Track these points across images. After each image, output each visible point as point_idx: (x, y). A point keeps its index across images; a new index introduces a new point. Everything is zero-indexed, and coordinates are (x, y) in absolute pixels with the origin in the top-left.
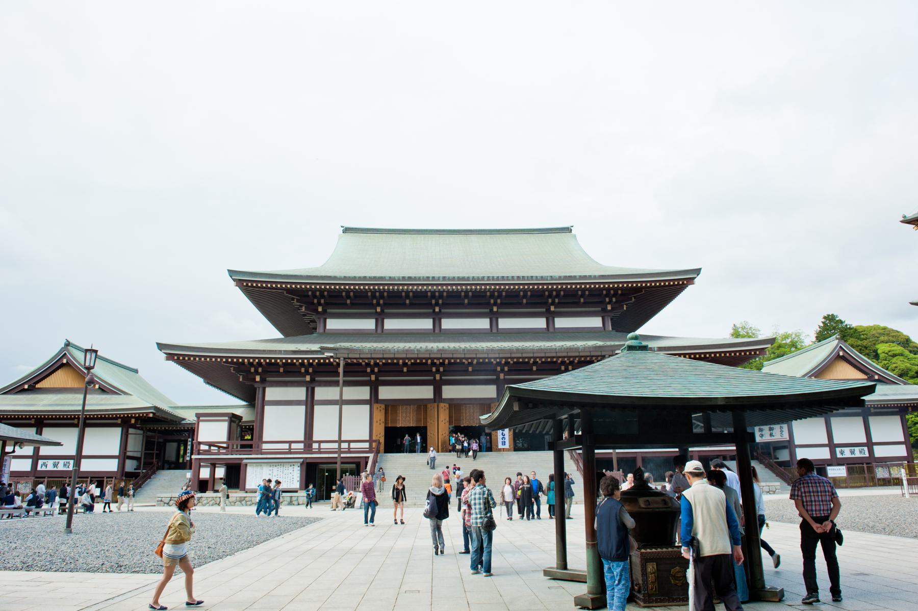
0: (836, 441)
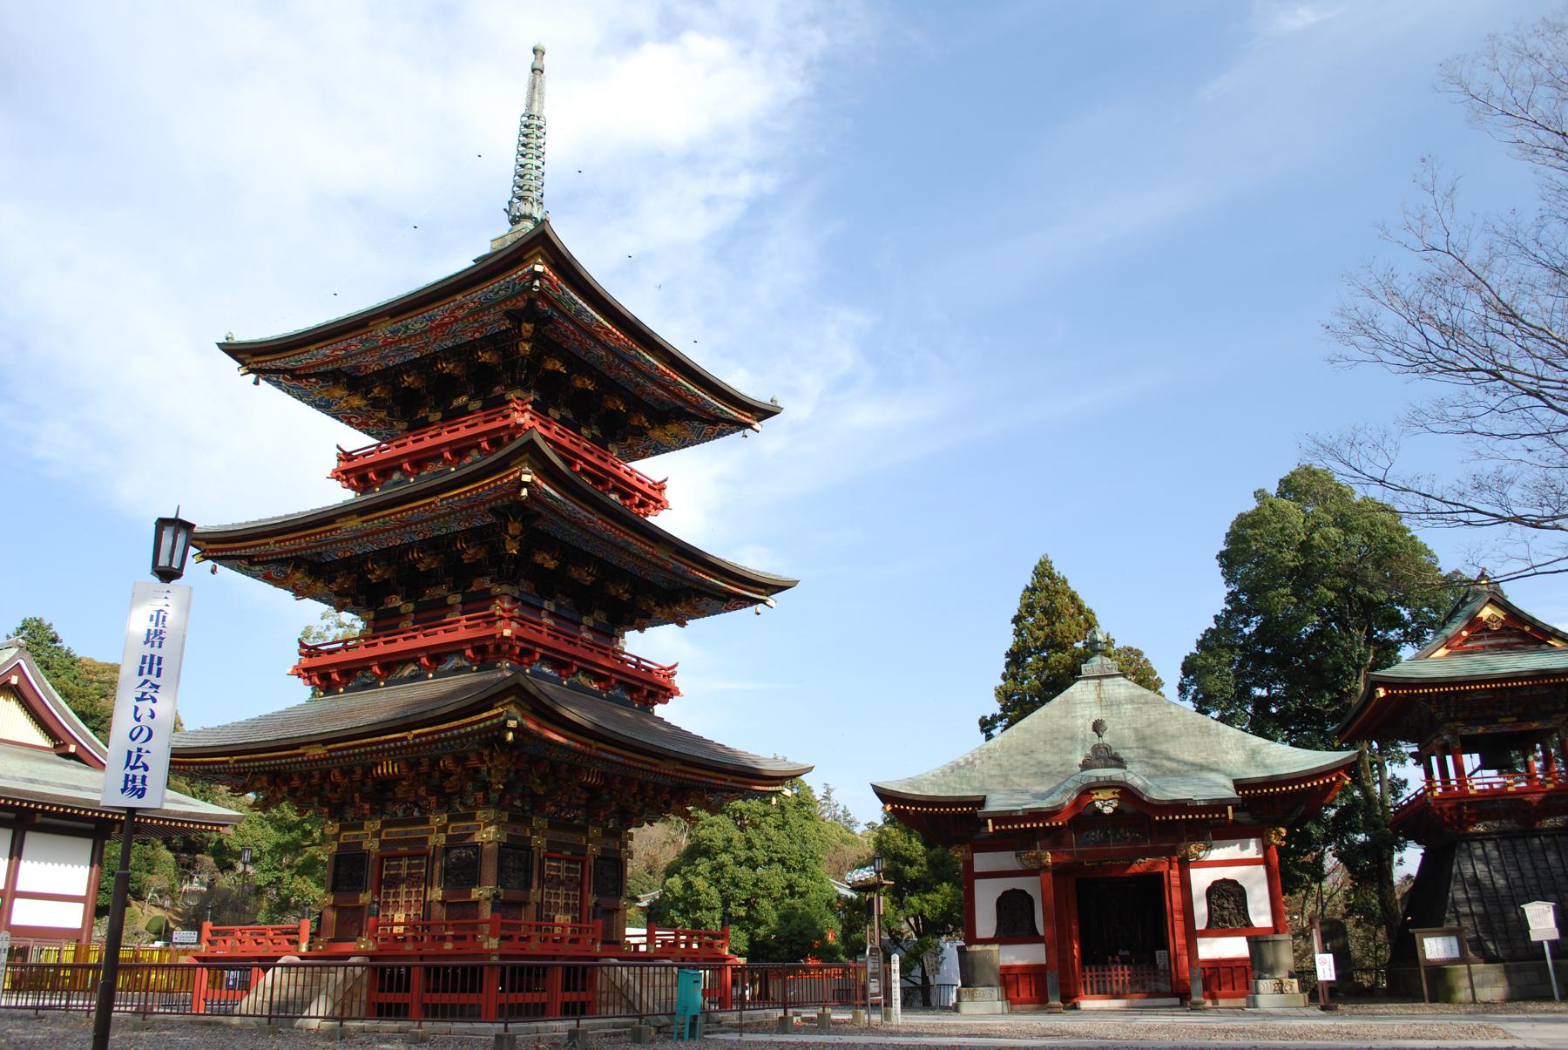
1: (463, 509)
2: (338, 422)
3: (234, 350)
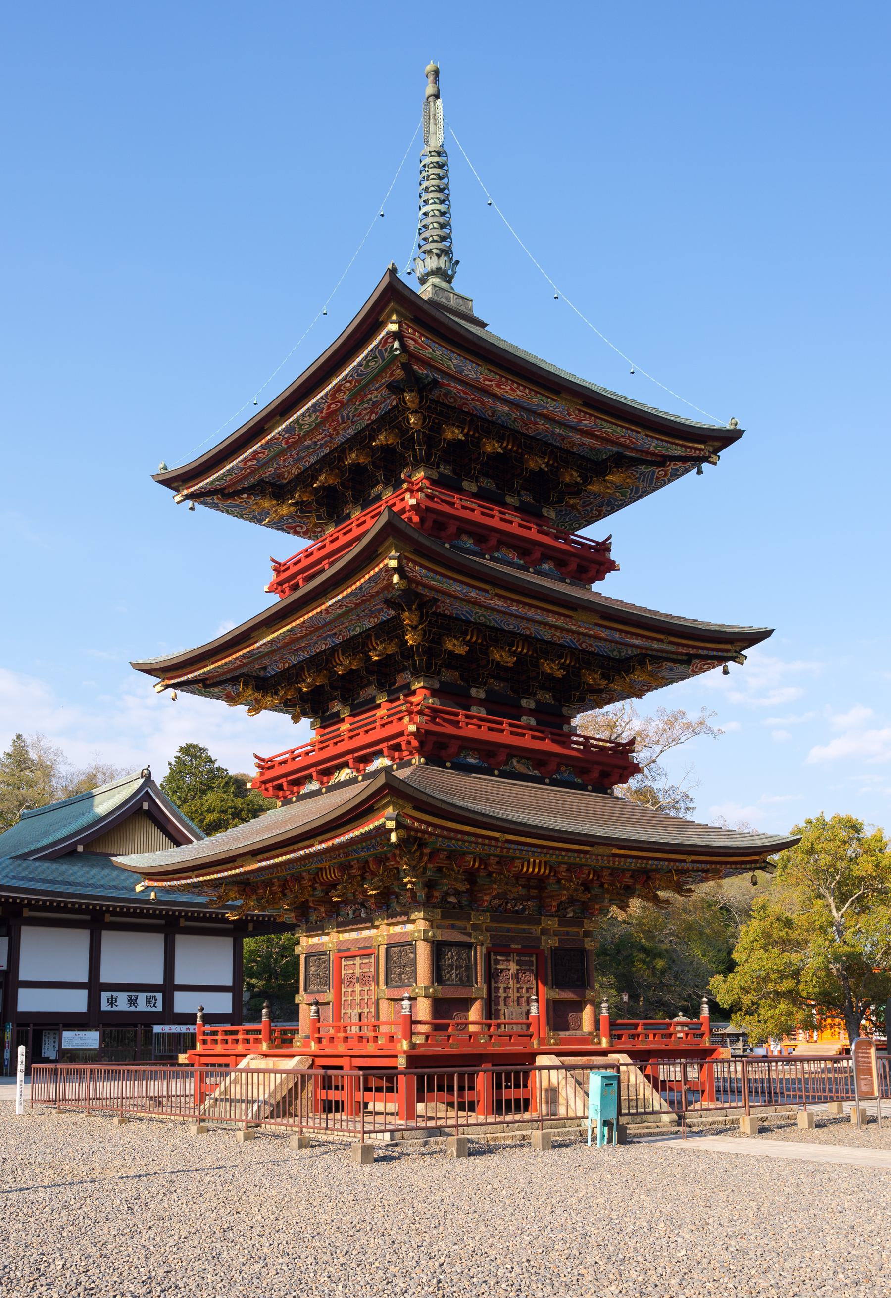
0: (106, 977)
1: (357, 605)
2: (285, 534)
3: (174, 482)
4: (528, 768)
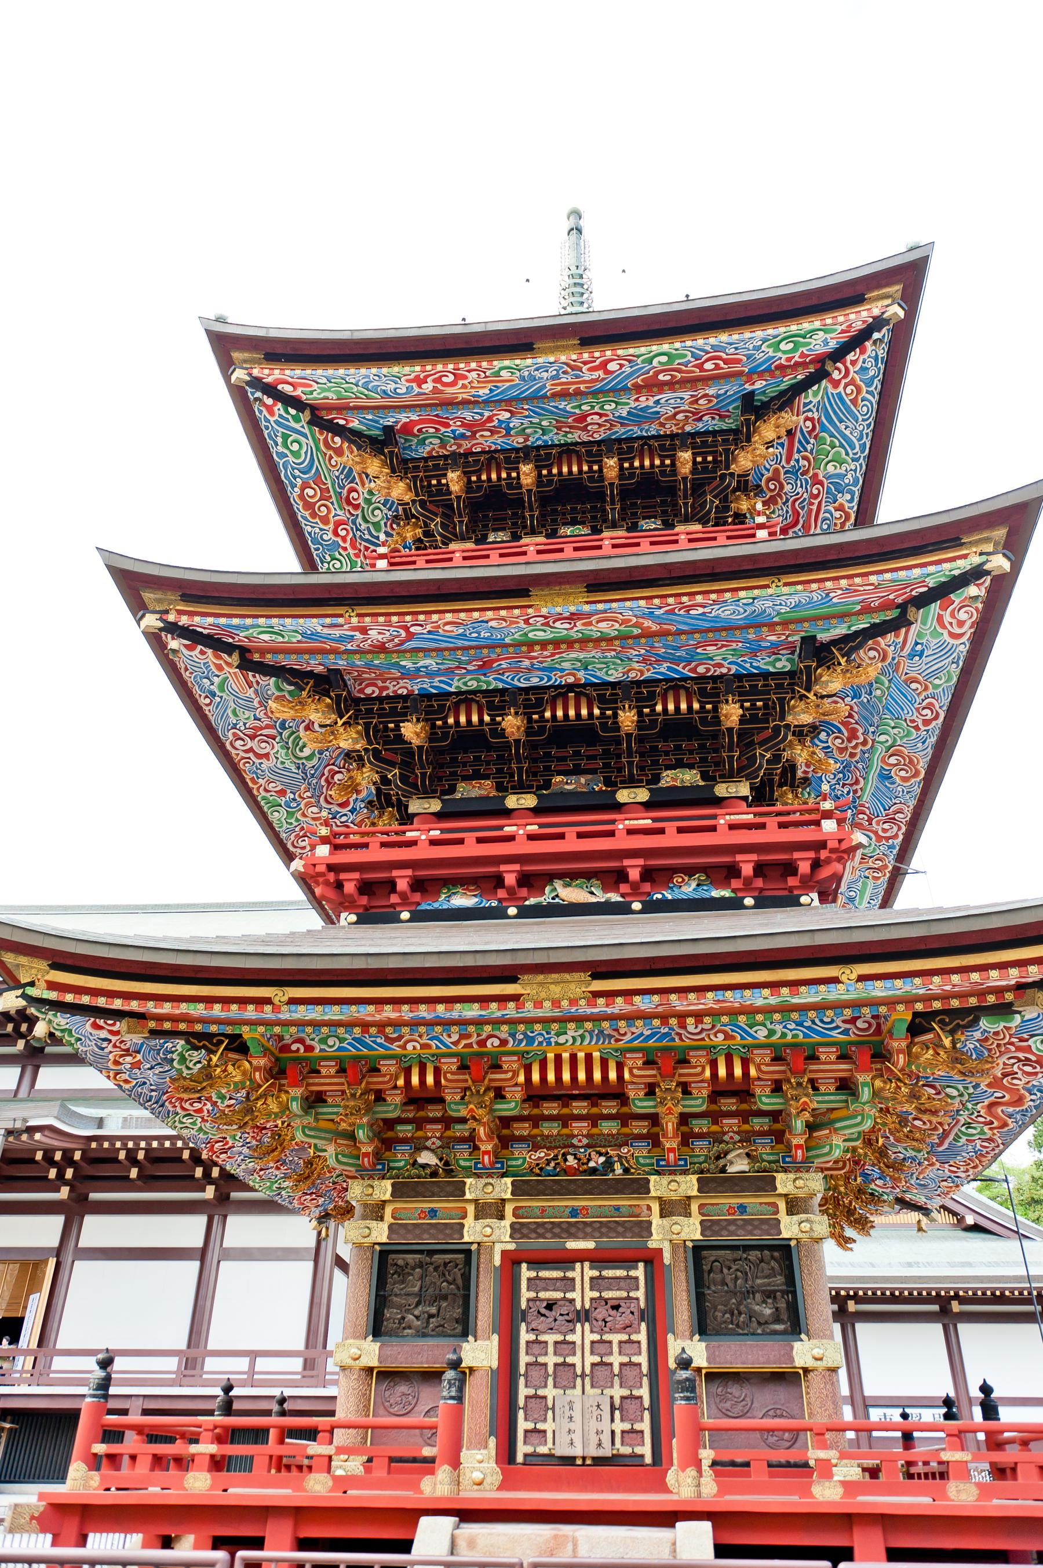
4: (592, 893)
